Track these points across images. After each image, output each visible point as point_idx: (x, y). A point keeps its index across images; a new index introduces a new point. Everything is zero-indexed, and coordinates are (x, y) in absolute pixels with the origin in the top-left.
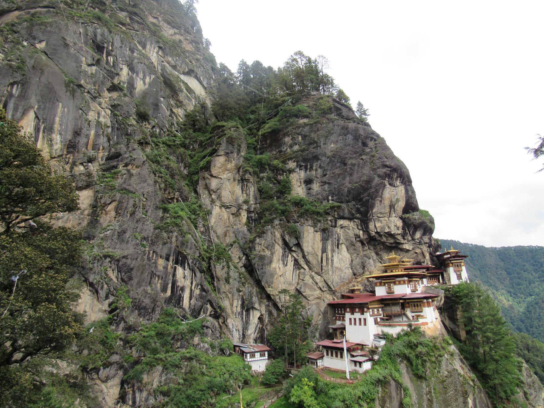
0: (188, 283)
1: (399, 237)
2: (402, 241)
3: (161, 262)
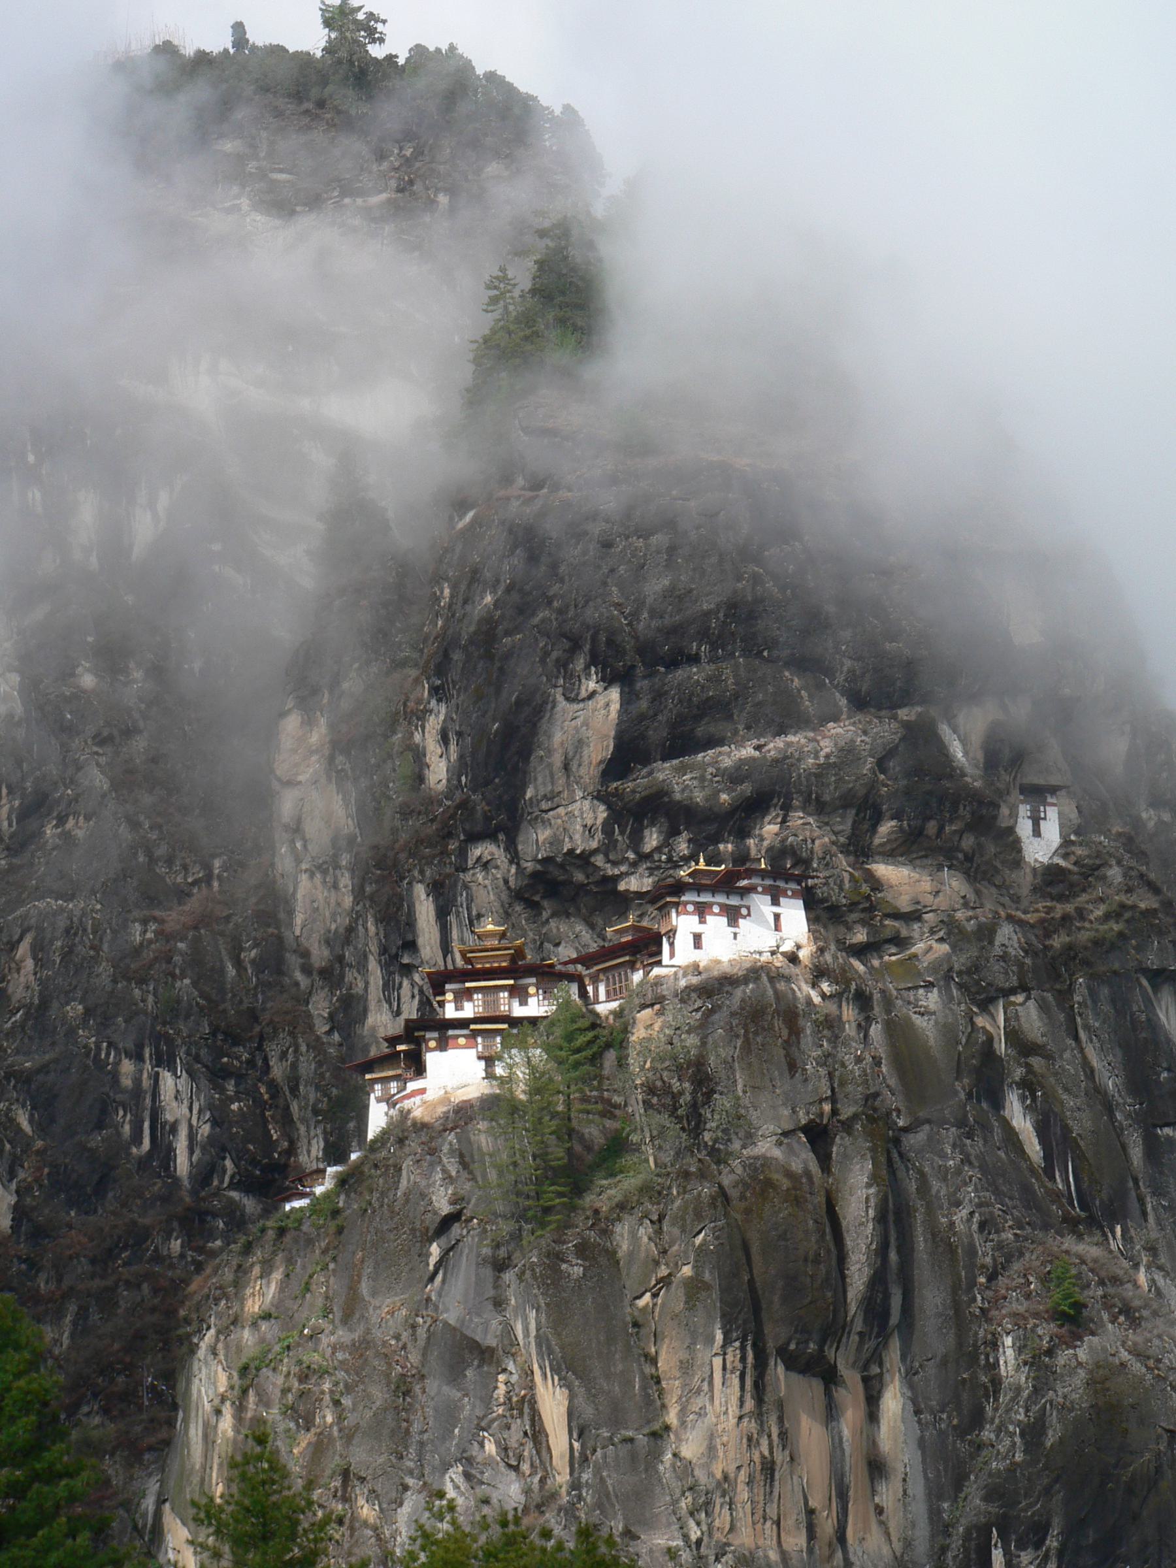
0: (186, 1111)
1: (599, 860)
2: (611, 871)
3: (127, 1067)
